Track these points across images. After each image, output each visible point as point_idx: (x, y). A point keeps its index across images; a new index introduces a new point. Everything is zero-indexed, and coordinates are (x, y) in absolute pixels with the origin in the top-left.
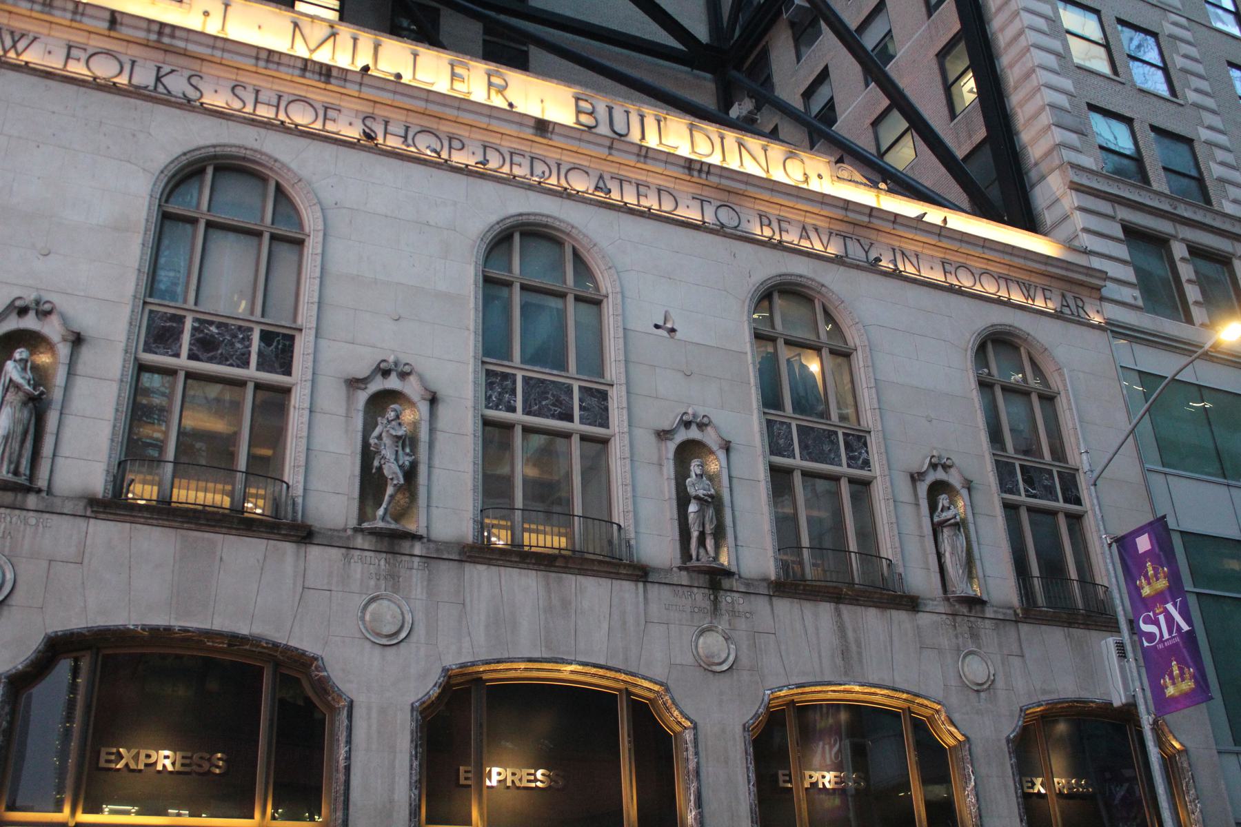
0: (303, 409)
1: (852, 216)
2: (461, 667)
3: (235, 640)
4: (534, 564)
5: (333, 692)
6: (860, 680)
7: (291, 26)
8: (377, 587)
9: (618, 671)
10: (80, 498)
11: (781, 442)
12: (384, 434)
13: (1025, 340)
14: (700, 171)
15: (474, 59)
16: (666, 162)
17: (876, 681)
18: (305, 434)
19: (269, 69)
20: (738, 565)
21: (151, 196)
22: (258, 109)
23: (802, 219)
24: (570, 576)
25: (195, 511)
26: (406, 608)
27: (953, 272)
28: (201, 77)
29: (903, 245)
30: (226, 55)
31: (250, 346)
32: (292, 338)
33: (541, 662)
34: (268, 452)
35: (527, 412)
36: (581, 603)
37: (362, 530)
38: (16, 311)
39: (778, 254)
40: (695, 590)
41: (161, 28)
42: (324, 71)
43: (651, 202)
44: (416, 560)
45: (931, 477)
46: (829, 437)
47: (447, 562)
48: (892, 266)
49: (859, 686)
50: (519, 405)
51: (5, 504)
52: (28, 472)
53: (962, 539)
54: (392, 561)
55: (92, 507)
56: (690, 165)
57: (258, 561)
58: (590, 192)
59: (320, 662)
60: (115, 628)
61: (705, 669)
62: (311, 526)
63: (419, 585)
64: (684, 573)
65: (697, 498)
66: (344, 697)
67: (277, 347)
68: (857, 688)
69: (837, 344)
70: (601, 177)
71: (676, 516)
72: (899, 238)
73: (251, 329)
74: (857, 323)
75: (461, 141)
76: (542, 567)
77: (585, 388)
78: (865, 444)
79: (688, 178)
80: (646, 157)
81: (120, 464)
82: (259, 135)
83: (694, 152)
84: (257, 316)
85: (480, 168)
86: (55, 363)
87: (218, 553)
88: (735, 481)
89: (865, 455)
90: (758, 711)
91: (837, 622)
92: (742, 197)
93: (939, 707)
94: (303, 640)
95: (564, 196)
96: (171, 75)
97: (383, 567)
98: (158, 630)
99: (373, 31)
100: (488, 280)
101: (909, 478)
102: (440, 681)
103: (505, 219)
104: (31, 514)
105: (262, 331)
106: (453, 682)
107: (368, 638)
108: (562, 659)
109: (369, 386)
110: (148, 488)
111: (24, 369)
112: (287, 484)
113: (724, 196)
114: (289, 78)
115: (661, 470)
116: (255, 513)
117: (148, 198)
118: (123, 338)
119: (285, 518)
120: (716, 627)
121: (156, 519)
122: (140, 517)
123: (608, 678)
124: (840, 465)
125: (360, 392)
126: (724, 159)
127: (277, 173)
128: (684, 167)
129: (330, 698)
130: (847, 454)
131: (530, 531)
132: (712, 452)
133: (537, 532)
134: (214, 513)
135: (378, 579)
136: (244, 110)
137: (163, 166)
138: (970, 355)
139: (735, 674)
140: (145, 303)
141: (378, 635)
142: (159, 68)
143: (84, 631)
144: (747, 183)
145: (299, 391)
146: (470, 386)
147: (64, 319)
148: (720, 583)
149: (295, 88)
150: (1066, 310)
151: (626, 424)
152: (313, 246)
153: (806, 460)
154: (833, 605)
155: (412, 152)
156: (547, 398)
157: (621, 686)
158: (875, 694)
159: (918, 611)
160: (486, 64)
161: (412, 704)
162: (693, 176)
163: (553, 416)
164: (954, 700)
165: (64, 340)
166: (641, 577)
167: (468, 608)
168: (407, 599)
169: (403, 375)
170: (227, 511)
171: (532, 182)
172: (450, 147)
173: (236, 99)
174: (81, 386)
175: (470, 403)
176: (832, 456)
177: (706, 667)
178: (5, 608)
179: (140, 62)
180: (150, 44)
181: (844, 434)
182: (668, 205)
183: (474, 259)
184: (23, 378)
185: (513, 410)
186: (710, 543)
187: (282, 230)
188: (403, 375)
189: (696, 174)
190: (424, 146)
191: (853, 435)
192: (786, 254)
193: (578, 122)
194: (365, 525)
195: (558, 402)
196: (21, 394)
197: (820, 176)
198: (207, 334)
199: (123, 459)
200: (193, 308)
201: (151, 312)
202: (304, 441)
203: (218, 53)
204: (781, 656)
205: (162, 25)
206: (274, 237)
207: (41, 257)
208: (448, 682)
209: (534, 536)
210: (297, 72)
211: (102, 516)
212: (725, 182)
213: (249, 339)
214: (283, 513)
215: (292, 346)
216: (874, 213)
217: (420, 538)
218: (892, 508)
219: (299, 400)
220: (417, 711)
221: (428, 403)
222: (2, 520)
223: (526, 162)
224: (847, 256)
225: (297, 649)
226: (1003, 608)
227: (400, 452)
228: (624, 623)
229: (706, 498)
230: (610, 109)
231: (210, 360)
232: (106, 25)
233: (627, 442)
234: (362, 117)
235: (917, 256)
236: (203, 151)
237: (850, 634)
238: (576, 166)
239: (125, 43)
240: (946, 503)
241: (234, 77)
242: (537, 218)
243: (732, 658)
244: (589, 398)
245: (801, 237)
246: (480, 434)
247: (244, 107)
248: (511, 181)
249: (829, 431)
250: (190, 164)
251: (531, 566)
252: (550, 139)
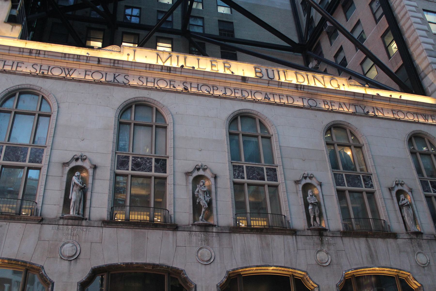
0: (171, 184)
1: (357, 98)
2: (233, 271)
3: (154, 266)
4: (256, 232)
5: (189, 282)
6: (378, 265)
7: (157, 55)
8: (201, 244)
9: (289, 268)
10: (100, 221)
11: (340, 181)
12: (199, 191)
13: (426, 135)
14: (301, 88)
15: (218, 59)
16: (288, 86)
17: (384, 265)
18: (173, 193)
19: (150, 70)
20: (329, 227)
21: (115, 117)
22: (148, 84)
23: (339, 101)
24: (269, 235)
25: (138, 222)
26: (212, 251)
27: (396, 114)
28: (128, 76)
29: (377, 106)
30: (136, 67)
31: (152, 164)
32: (166, 160)
33: (261, 267)
34: (161, 200)
35: (248, 178)
36: (273, 244)
37: (195, 225)
38: (75, 160)
39: (332, 114)
40: (314, 237)
41: (114, 61)
42: (168, 69)
43: (284, 101)
44: (214, 233)
45: (397, 189)
46: (357, 177)
47: (225, 234)
48: (373, 114)
49: (378, 267)
50: (245, 176)
51: (75, 224)
52: (82, 213)
53: (411, 211)
54: (206, 235)
55: (103, 224)
56: (297, 86)
57: (160, 238)
58: (263, 99)
59: (184, 272)
60: (114, 264)
61: (320, 265)
62: (177, 224)
63: (216, 242)
64: (309, 231)
65: (312, 204)
66: (193, 283)
67: (161, 164)
68: (377, 269)
69: (357, 144)
70: (266, 94)
71: (304, 211)
72: (375, 104)
73: (152, 159)
74: (363, 136)
75: (217, 87)
76: (259, 233)
77: (268, 168)
78: (371, 179)
79: (297, 91)
80: (281, 85)
81: (112, 208)
82: (149, 92)
83: (298, 82)
84: (153, 154)
85: (224, 96)
86: (88, 176)
87: (147, 236)
88: (324, 197)
89: (371, 183)
90: (341, 279)
91: (367, 244)
92: (317, 95)
93: (409, 274)
94: (177, 264)
95: (254, 102)
96: (118, 76)
97: (203, 237)
98: (128, 264)
99: (184, 54)
100: (230, 134)
101: (388, 190)
102: (226, 276)
103: (234, 112)
104: (84, 227)
105: (155, 159)
106: (231, 276)
107: (199, 262)
108: (269, 265)
109: (193, 174)
110: (121, 215)
111: (79, 179)
112: (168, 211)
113: (310, 96)
114: (157, 72)
115: (298, 195)
116: (158, 221)
117: (114, 117)
118: (110, 165)
119: (168, 222)
120: (323, 250)
121: (125, 226)
122: (120, 226)
123: (286, 271)
124: (362, 187)
125: (190, 177)
126: (309, 83)
127: (156, 105)
128: (295, 87)
129: (188, 284)
130: (364, 183)
131: (253, 220)
132: (315, 187)
133: (256, 220)
134: (144, 222)
135: (202, 241)
136: (143, 85)
137: (119, 106)
138: (406, 143)
139: (331, 267)
140: (116, 153)
141: (203, 261)
142: (115, 74)
143: (104, 266)
144: (318, 90)
145: (169, 178)
146: (228, 171)
147: (90, 161)
148: (323, 234)
149: (159, 76)
151: (283, 179)
152: (170, 128)
153: (349, 186)
154: (365, 239)
155: (201, 93)
156: (255, 173)
157: (290, 273)
158: (384, 270)
159: (397, 238)
160: (223, 60)
161: (217, 285)
162: (298, 90)
163: (258, 179)
164: (415, 271)
165: (91, 168)
167: (234, 250)
168: (212, 248)
169: (204, 170)
170: (148, 222)
171: (242, 98)
172: (213, 90)
173: (140, 81)
174: (97, 182)
175: (228, 177)
176: (359, 184)
177: (321, 264)
178: (78, 260)
179: (108, 73)
180: (111, 67)
181: (363, 176)
182: (290, 101)
183: (225, 127)
184: (78, 182)
185: (243, 178)
186: (318, 219)
187: (159, 124)
188: (204, 170)
189: (299, 89)
190: (204, 90)
191: (366, 176)
192: (334, 114)
193: (256, 76)
194: (196, 223)
195: (259, 174)
196: (78, 187)
197: (344, 85)
198: (137, 161)
199: (112, 206)
200: (132, 153)
201: (118, 156)
202: (173, 195)
203: (133, 67)
204: (348, 259)
205: (115, 60)
206: (157, 127)
207: (81, 141)
208: (229, 276)
209: (255, 222)
210: (160, 70)
211: (107, 226)
212: (310, 91)
213: (151, 162)
214: (167, 222)
215: (166, 163)
216: (365, 96)
217: (215, 226)
218: (383, 201)
219: (169, 181)
220: (219, 287)
221: (214, 178)
222: (75, 230)
223: (240, 92)
224: (356, 112)
225: (176, 268)
226: (430, 235)
227: (206, 196)
228: (290, 251)
230: (267, 70)
231: (139, 170)
232: (97, 62)
233: (284, 186)
234: (182, 83)
235: (382, 109)
236: (131, 100)
237: (372, 248)
238: (257, 91)
239: (103, 68)
240: (403, 198)
241: (139, 75)
242: (245, 110)
243: (329, 261)
244: (269, 171)
245: (339, 107)
246: (233, 187)
247: (143, 84)
248: (235, 99)
249: (357, 175)
250: (127, 105)
251: (255, 233)
252: (247, 83)
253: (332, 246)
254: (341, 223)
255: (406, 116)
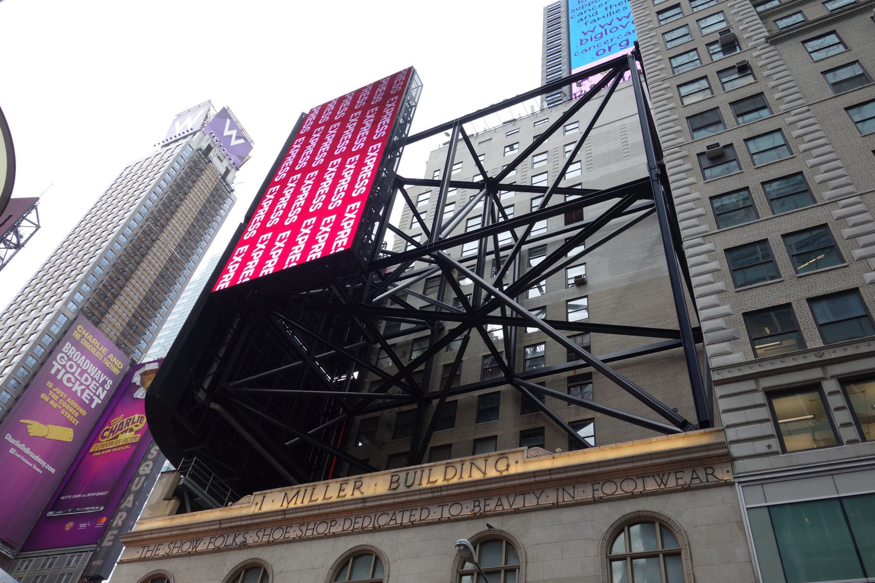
27: (600, 490)
150: (697, 481)
255: (619, 489)
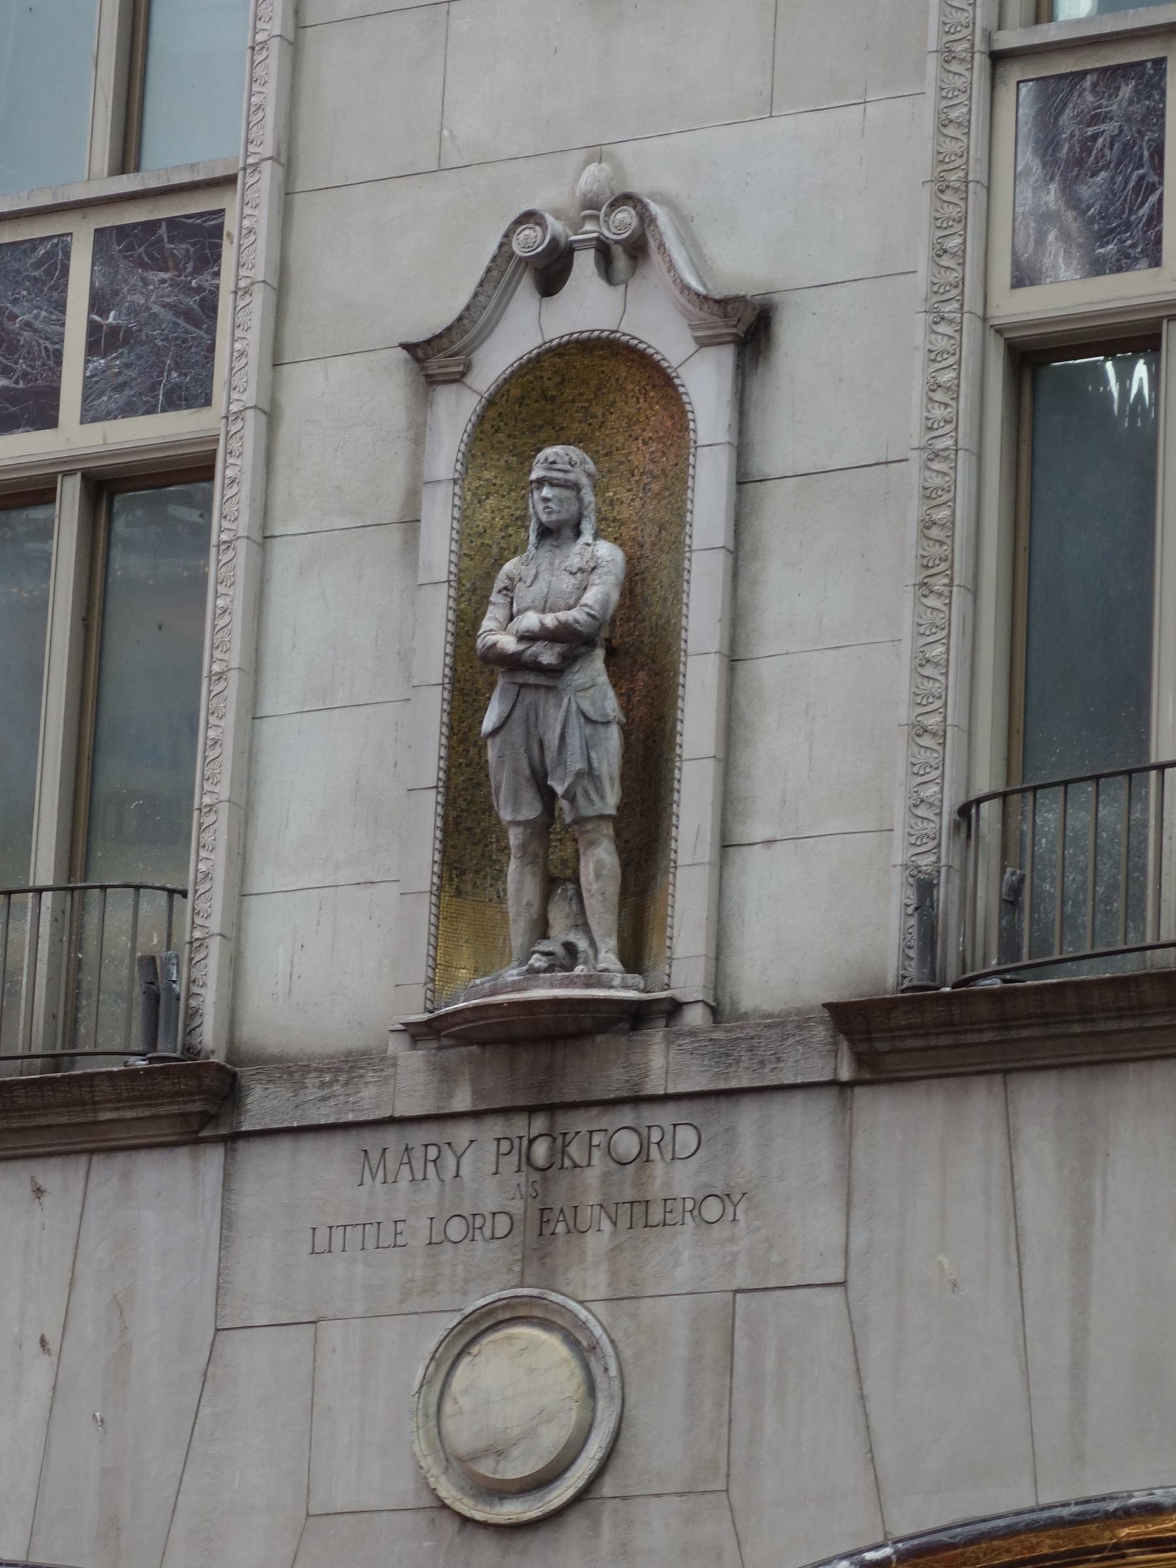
40: (463, 1133)
77: (122, 231)
139: (606, 1527)
166: (207, 1119)
229: (536, 648)
253: (688, 1231)
254: (897, 878)
